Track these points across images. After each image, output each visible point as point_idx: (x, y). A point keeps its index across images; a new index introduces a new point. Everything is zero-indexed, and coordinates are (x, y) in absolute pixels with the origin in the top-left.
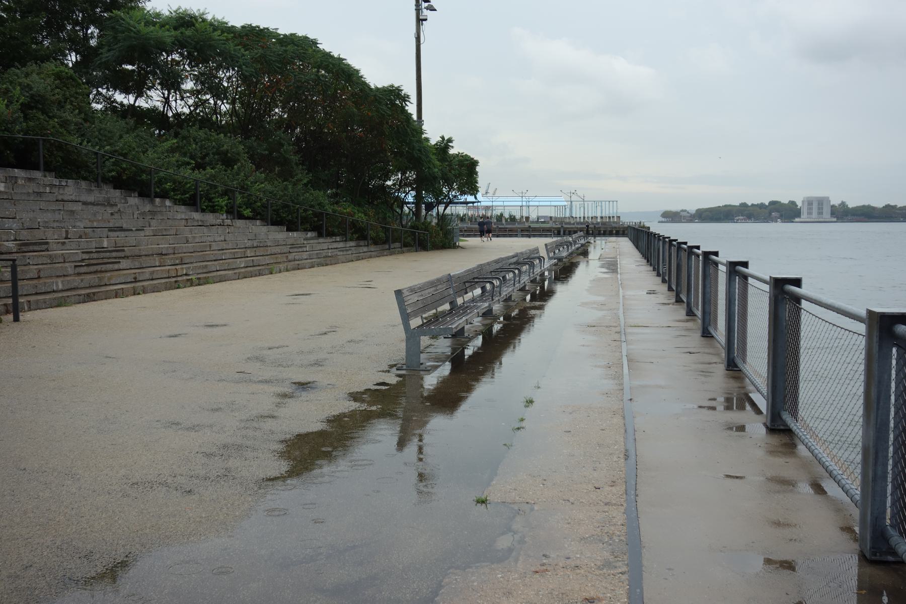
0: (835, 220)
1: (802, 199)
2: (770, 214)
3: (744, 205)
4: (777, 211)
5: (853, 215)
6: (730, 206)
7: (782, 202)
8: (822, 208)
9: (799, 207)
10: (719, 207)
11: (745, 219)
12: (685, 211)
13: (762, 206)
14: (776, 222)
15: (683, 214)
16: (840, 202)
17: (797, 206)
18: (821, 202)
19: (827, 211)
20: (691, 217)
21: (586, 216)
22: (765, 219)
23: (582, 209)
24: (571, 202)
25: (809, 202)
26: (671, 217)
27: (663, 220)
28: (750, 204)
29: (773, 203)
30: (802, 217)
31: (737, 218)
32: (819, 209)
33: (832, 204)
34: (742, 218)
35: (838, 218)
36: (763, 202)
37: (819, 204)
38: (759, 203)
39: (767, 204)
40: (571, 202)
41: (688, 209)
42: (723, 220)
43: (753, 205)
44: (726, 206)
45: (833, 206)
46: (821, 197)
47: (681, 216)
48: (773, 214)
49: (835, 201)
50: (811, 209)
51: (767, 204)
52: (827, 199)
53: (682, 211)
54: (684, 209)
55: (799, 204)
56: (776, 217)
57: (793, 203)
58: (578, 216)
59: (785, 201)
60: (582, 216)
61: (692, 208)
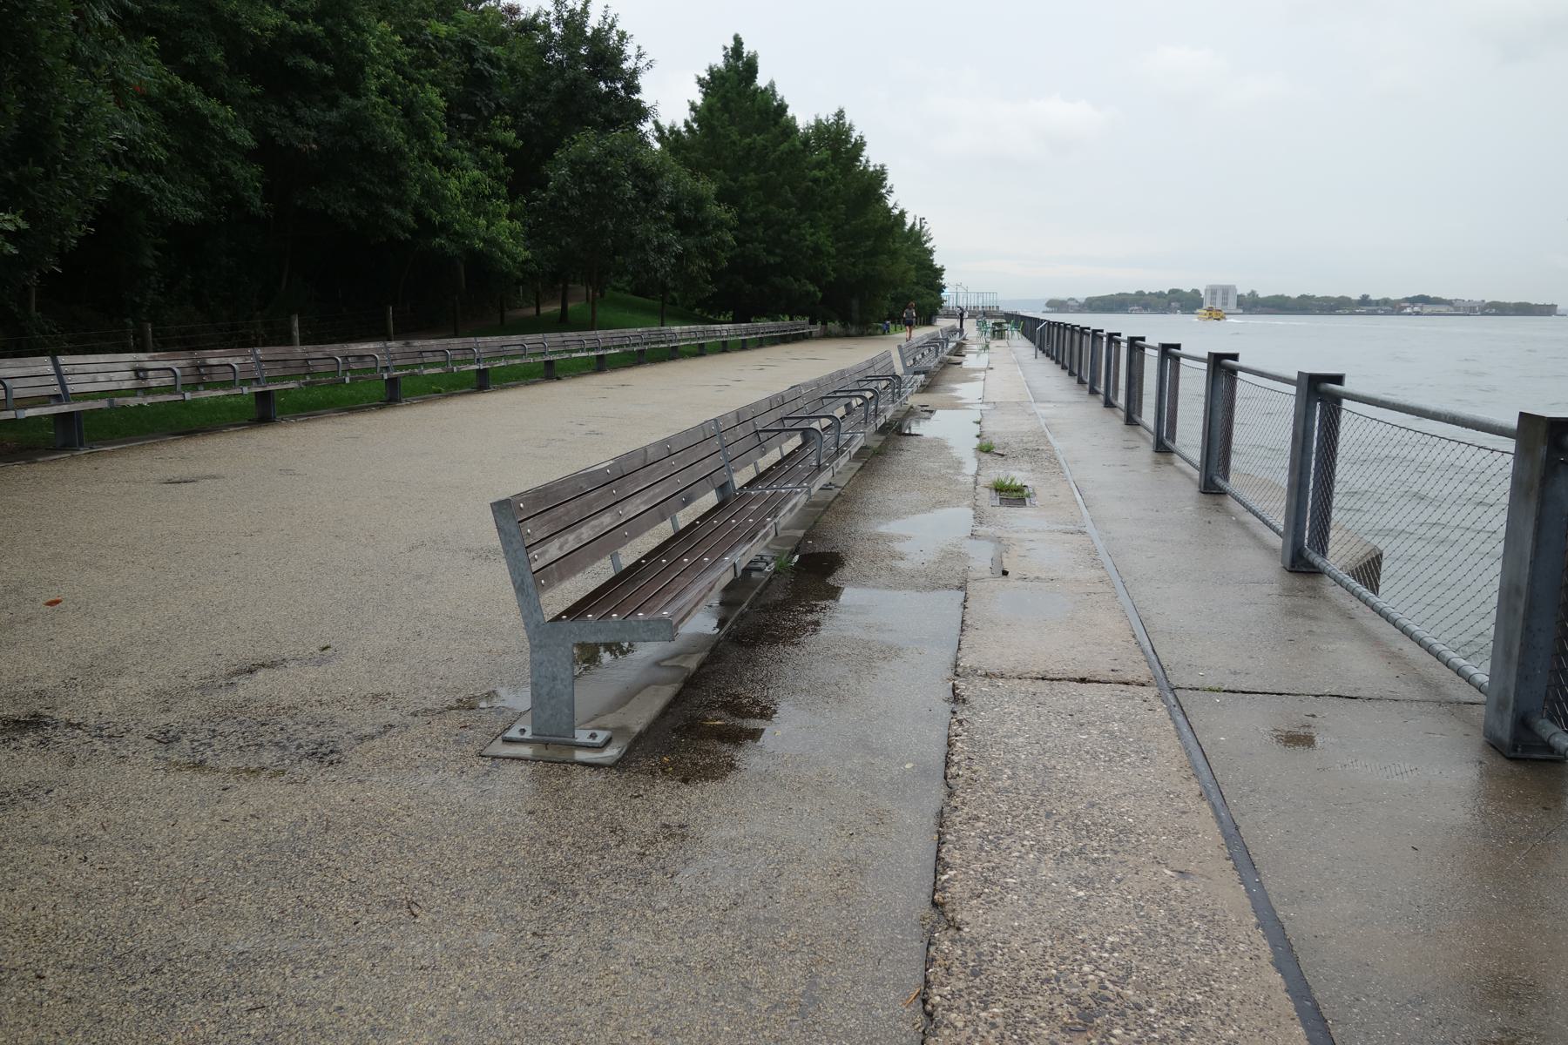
0: (1241, 311)
2: (1169, 304)
5: (1263, 306)
6: (1125, 294)
7: (1185, 290)
8: (1227, 299)
10: (1112, 295)
13: (1160, 295)
14: (1176, 313)
15: (1070, 303)
16: (1249, 291)
18: (1226, 291)
19: (1232, 301)
22: (1163, 310)
25: (1213, 291)
26: (1057, 305)
27: (1048, 309)
29: (1173, 292)
33: (1239, 293)
34: (1136, 308)
35: (1244, 309)
36: (1162, 290)
37: (1223, 294)
44: (1120, 294)
48: (1173, 304)
49: (1243, 290)
51: (1166, 292)
52: (1233, 288)
55: (1202, 293)
57: (1196, 292)
61: (1081, 296)
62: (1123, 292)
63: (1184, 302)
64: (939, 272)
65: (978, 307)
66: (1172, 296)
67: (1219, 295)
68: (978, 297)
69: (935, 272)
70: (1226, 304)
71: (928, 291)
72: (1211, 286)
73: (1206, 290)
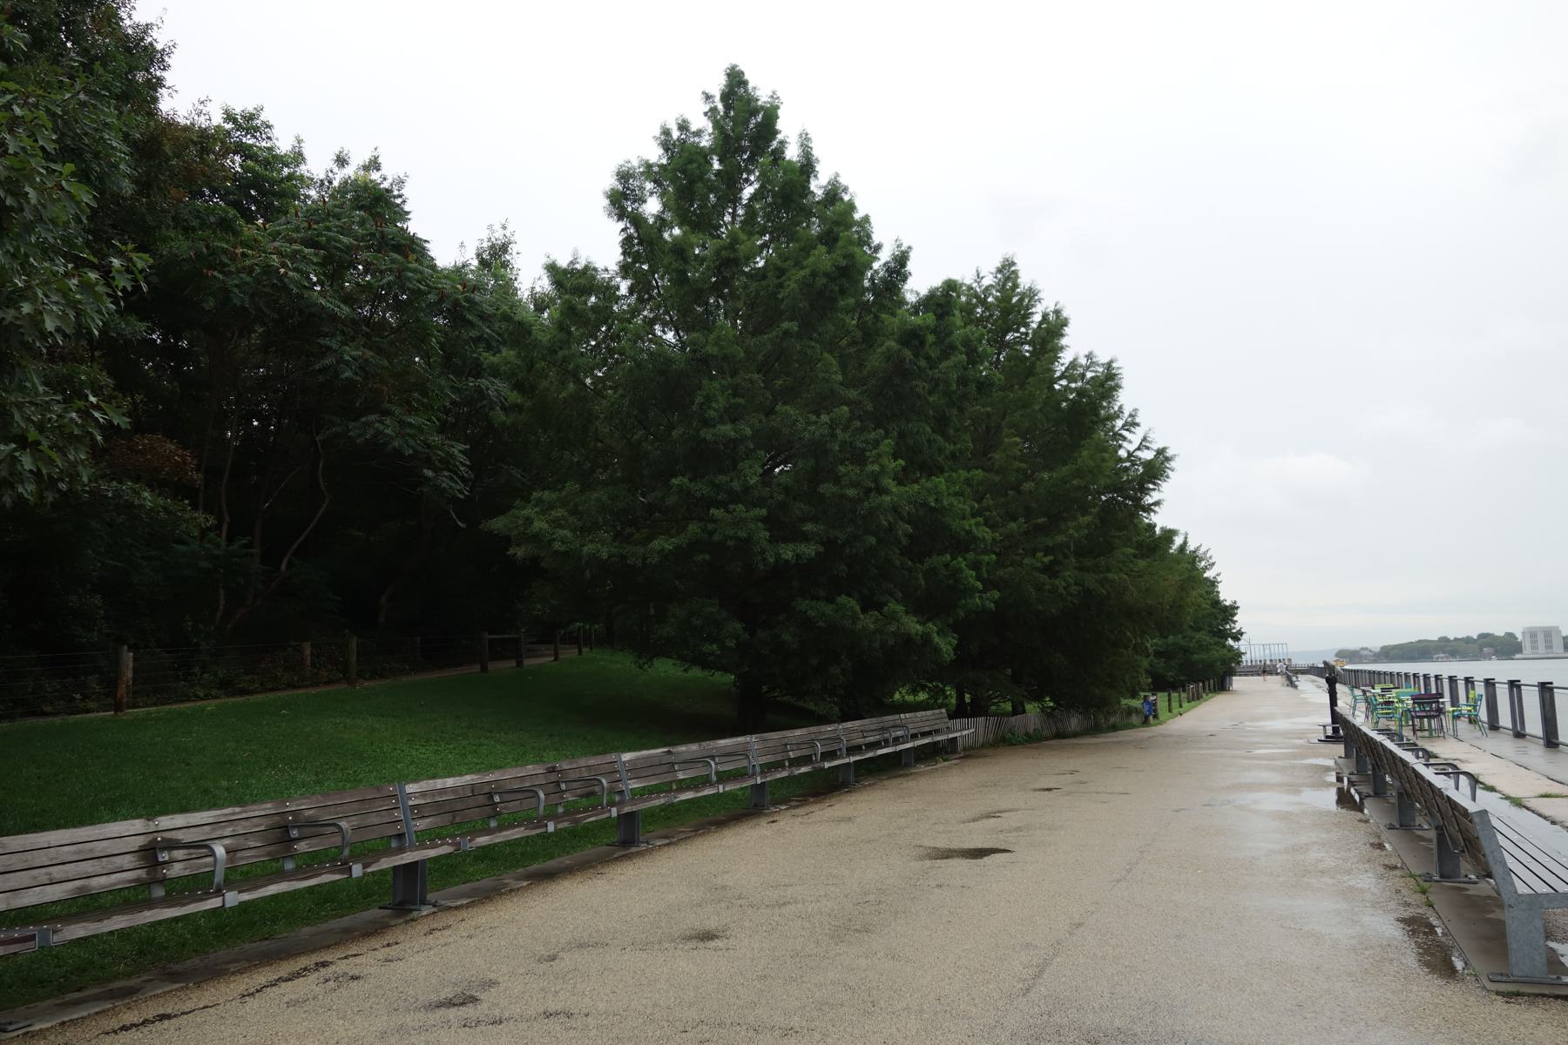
1: (1522, 630)
4: (1490, 645)
9: (1519, 640)
12: (1367, 649)
13: (1468, 640)
14: (1490, 659)
25: (1533, 634)
28: (1452, 639)
29: (1483, 636)
30: (1524, 652)
31: (1437, 656)
32: (1546, 641)
37: (1531, 636)
39: (1475, 637)
42: (1418, 658)
43: (1456, 639)
46: (1546, 628)
48: (1485, 649)
50: (1536, 642)
51: (1475, 637)
52: (1557, 630)
54: (1364, 646)
56: (1489, 653)
57: (1511, 635)
59: (1500, 633)
63: (1506, 647)
64: (1229, 612)
65: (1265, 661)
67: (1540, 638)
68: (1264, 650)
69: (1224, 612)
70: (1551, 647)
71: (1216, 639)
73: (1523, 633)
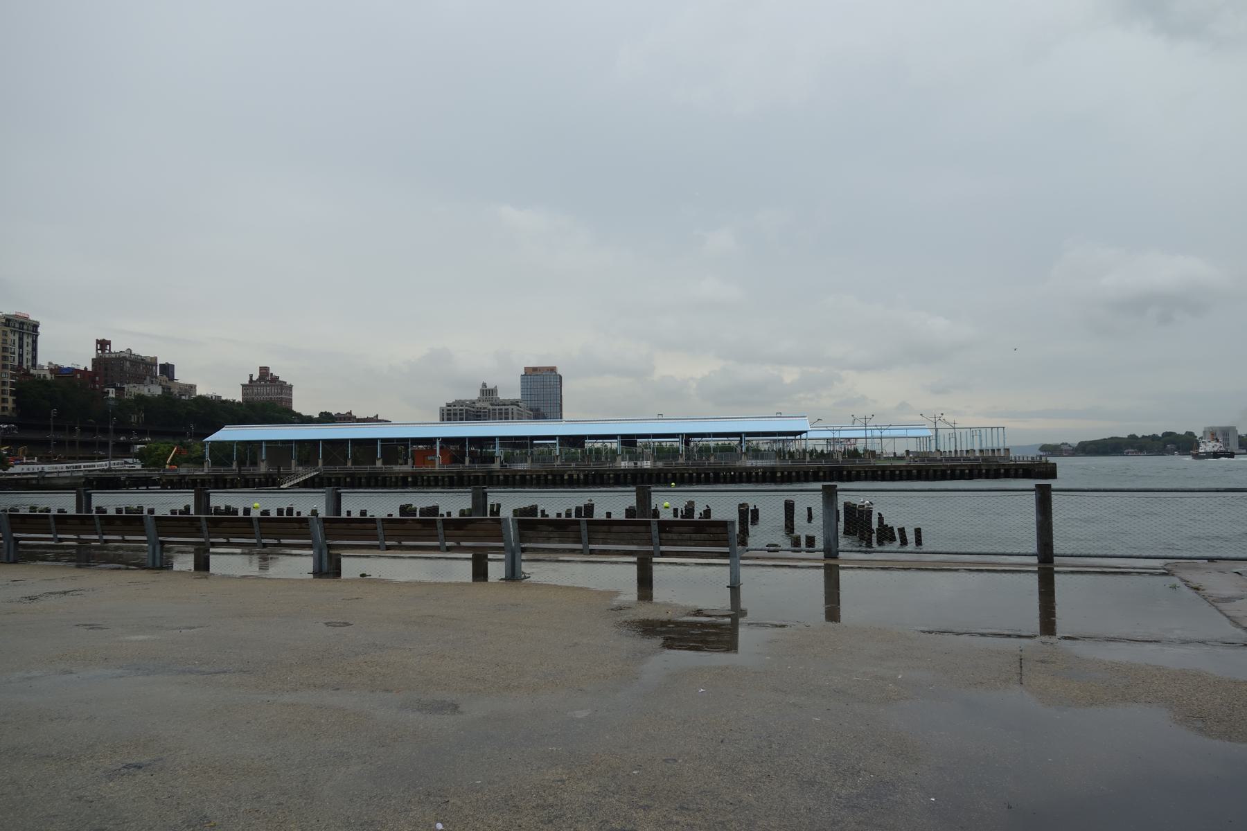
3: (1133, 437)
4: (1173, 443)
11: (1136, 452)
12: (1066, 444)
13: (1154, 437)
17: (1196, 437)
20: (1072, 450)
21: (959, 449)
22: (1160, 452)
23: (953, 440)
24: (937, 429)
31: (1126, 451)
34: (1132, 450)
38: (1151, 434)
39: (1160, 435)
40: (937, 429)
41: (1069, 442)
43: (1143, 437)
44: (1112, 438)
45: (1239, 437)
47: (1062, 450)
51: (1160, 435)
52: (1233, 429)
53: (1063, 444)
55: (1199, 434)
57: (1190, 434)
58: (947, 450)
60: (953, 450)
61: (1074, 441)
62: (1115, 436)
66: (1168, 438)
72: (1209, 428)
73: (1204, 432)
